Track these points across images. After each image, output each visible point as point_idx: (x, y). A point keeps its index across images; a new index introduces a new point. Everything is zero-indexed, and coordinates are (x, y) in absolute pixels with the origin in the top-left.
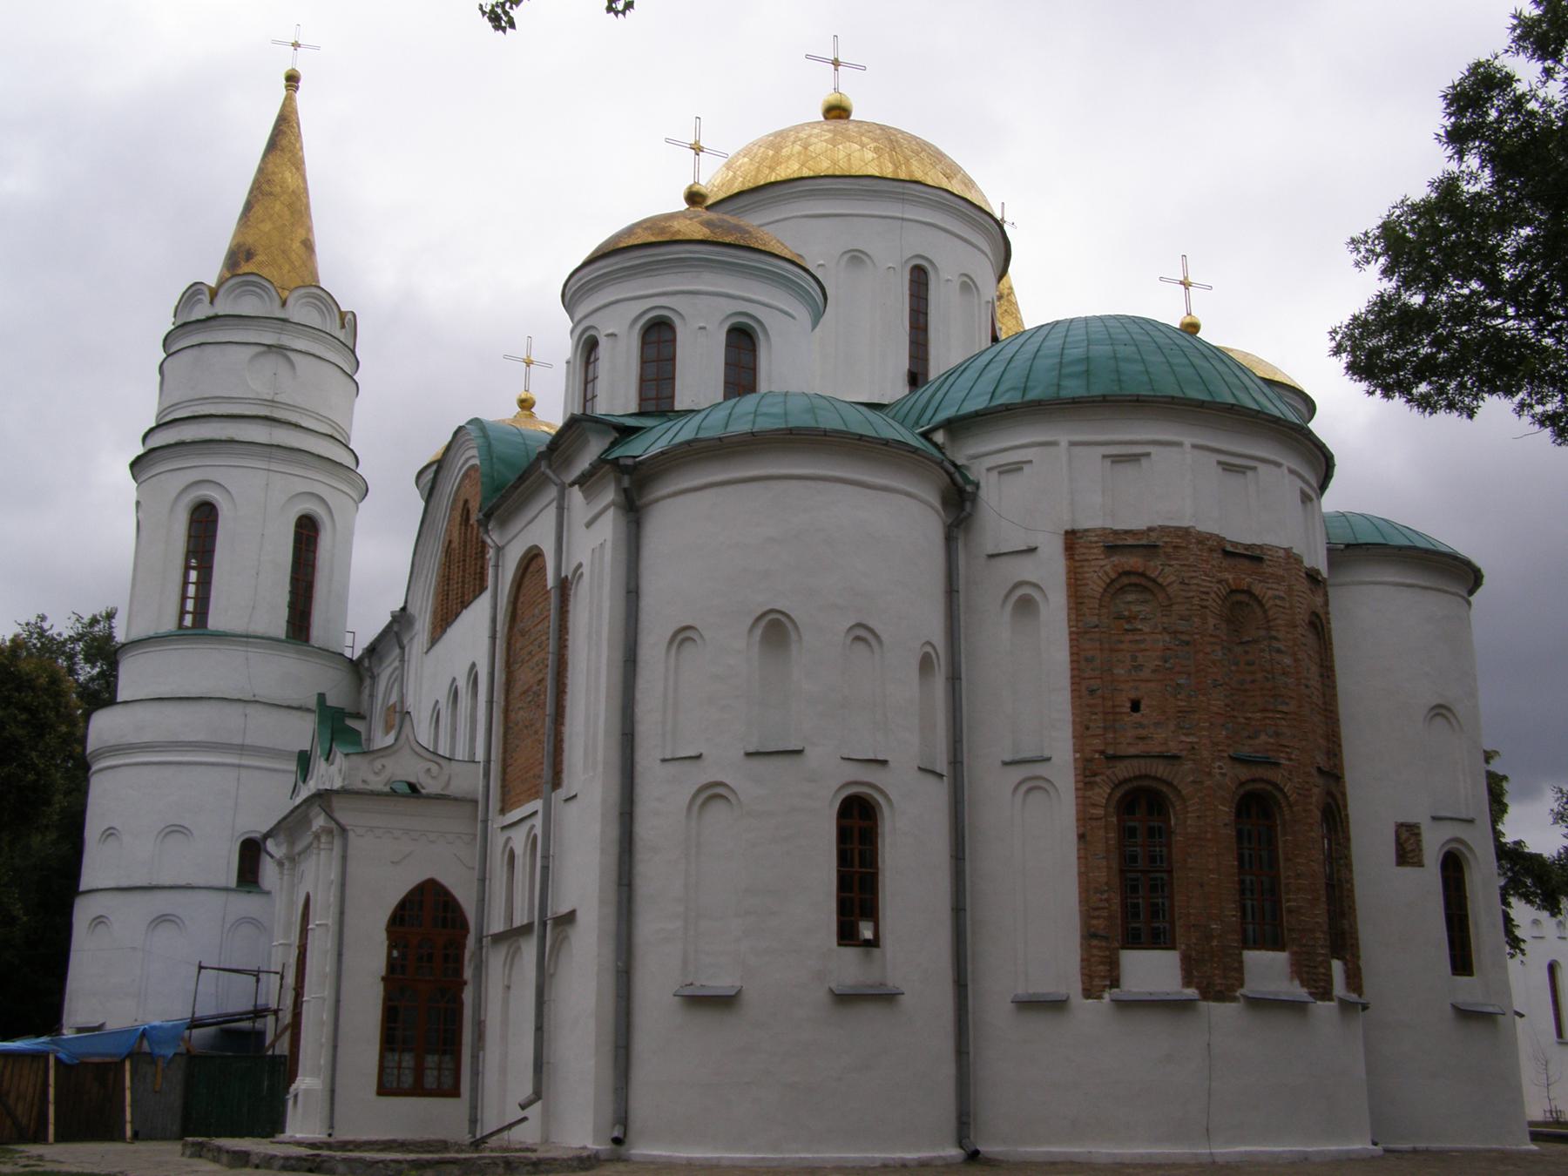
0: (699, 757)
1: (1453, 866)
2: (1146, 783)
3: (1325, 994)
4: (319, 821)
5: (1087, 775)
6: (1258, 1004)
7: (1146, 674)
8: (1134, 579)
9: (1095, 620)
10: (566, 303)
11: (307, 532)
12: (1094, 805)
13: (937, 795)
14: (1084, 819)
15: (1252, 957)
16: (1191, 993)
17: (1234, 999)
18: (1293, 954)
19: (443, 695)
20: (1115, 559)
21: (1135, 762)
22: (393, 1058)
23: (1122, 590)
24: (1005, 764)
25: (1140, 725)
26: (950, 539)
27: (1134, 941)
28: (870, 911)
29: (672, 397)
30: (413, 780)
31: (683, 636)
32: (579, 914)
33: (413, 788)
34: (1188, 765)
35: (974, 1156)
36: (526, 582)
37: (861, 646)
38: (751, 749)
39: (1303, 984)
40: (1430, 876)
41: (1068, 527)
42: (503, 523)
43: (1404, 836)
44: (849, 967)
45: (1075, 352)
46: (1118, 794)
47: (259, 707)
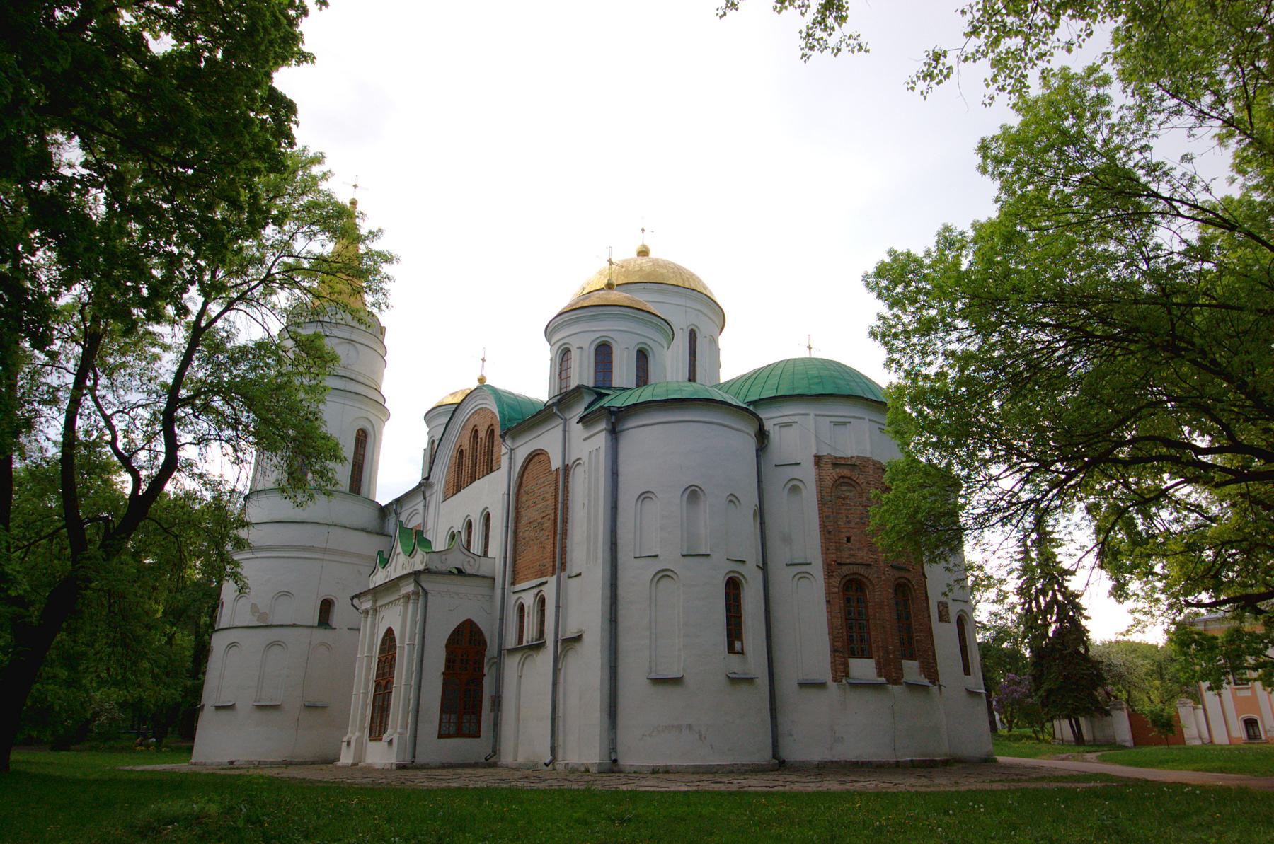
0: (656, 556)
2: (856, 577)
4: (409, 588)
5: (829, 572)
7: (852, 525)
8: (846, 480)
9: (829, 498)
10: (548, 332)
12: (834, 587)
14: (828, 593)
16: (882, 680)
17: (900, 684)
18: (922, 662)
19: (459, 526)
20: (837, 470)
21: (851, 566)
23: (841, 485)
24: (787, 565)
25: (850, 549)
26: (758, 456)
27: (853, 655)
28: (740, 638)
29: (611, 381)
30: (460, 567)
31: (645, 496)
32: (584, 636)
33: (457, 569)
34: (875, 569)
35: (782, 763)
36: (530, 466)
37: (731, 504)
38: (685, 553)
41: (814, 452)
44: (735, 663)
45: (815, 373)
46: (843, 582)
47: (336, 528)
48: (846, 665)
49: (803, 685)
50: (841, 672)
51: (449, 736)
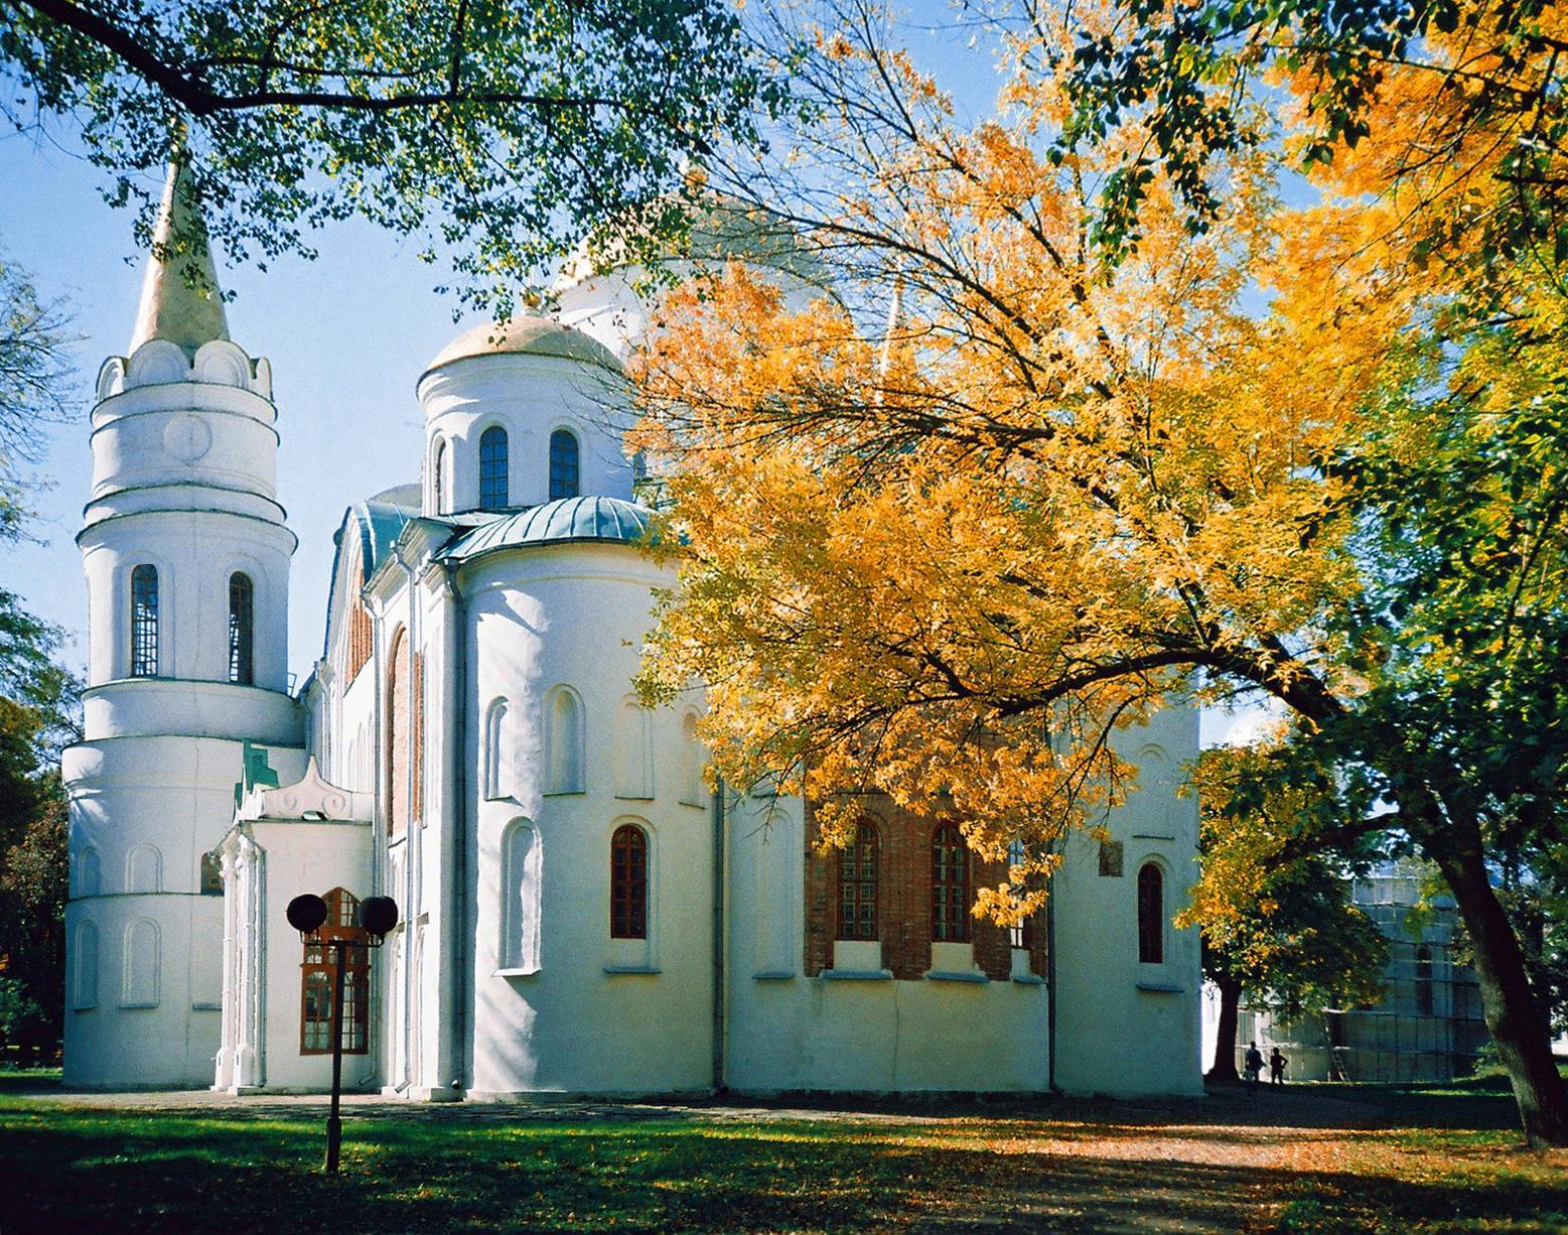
1: (1150, 879)
3: (1004, 977)
6: (942, 979)
11: (241, 590)
13: (702, 823)
15: (938, 948)
16: (888, 973)
17: (922, 979)
18: (976, 945)
22: (310, 1026)
31: (499, 705)
39: (982, 967)
40: (1127, 886)
42: (385, 599)
43: (1109, 851)
48: (829, 952)
49: (767, 979)
50: (819, 960)
51: (315, 1051)
